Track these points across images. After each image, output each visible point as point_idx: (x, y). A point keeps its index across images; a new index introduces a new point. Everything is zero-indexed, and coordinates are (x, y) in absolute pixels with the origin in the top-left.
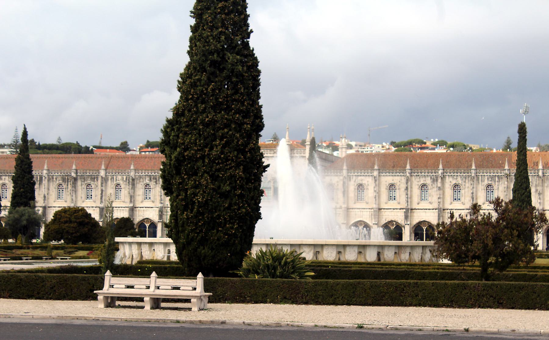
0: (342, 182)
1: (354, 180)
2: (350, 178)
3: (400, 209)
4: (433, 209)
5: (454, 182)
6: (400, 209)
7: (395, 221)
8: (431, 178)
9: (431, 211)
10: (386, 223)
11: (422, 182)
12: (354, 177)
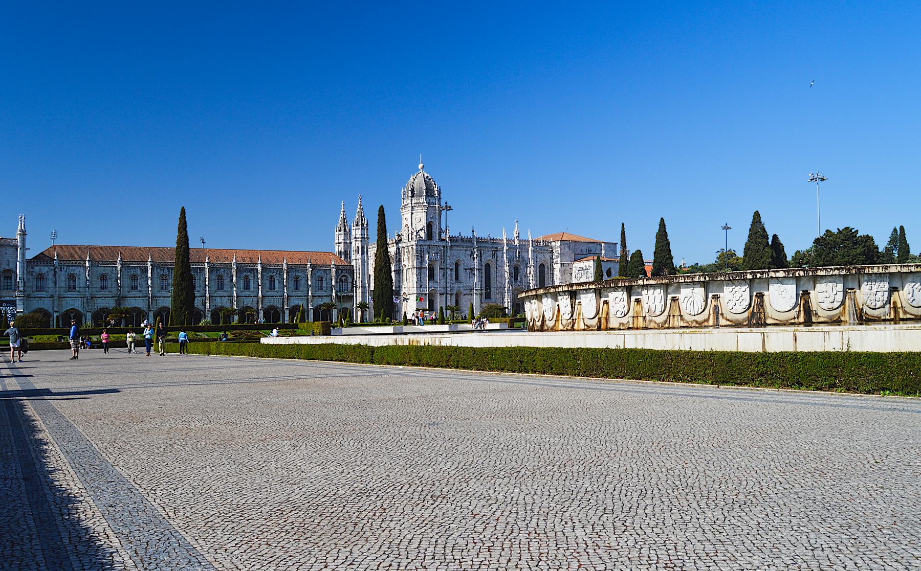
0: (53, 272)
1: (65, 270)
2: (61, 268)
3: (111, 297)
4: (142, 297)
5: (162, 273)
6: (111, 297)
7: (106, 308)
8: (140, 269)
9: (141, 298)
10: (97, 311)
11: (132, 273)
12: (65, 267)
